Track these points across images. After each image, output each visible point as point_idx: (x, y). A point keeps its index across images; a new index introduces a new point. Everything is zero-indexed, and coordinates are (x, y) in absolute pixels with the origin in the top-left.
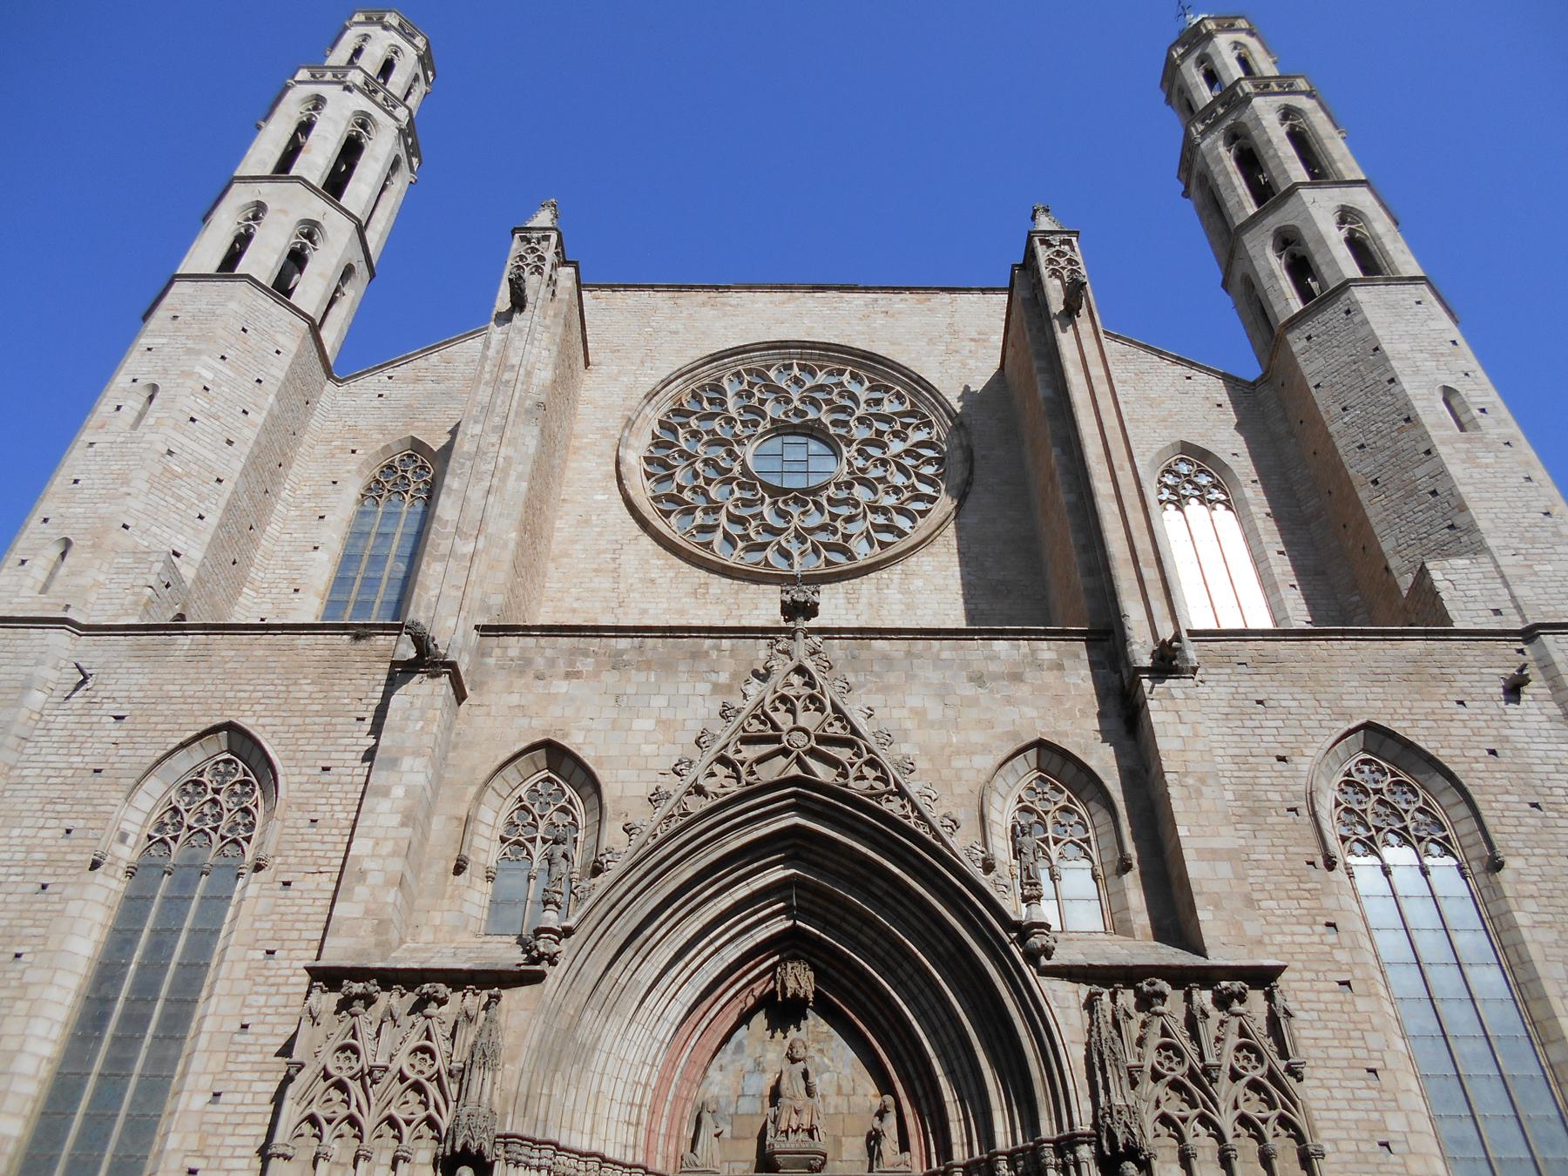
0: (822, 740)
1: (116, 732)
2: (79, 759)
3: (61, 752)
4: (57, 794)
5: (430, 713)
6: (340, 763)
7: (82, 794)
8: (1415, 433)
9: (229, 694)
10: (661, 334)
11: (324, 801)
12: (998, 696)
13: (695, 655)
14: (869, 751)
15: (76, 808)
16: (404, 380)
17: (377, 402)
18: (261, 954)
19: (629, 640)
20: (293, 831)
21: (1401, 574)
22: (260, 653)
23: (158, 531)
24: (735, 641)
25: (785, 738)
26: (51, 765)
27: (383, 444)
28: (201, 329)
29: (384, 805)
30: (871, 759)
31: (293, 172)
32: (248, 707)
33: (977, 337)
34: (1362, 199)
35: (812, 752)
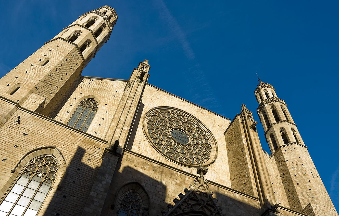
0: (207, 204)
1: (23, 138)
2: (12, 141)
3: (7, 137)
4: (4, 148)
5: (114, 165)
6: (82, 169)
7: (11, 151)
8: (307, 176)
9: (55, 140)
10: (155, 98)
11: (77, 177)
12: (237, 206)
13: (172, 174)
14: (218, 211)
15: (8, 154)
16: (96, 83)
17: (89, 85)
18: (55, 214)
19: (157, 165)
20: (68, 182)
21: (302, 204)
22: (65, 133)
23: (42, 92)
24: (181, 174)
25: (199, 201)
26: (3, 139)
27: (88, 95)
28: (64, 51)
29: (100, 185)
30: (218, 212)
31: (89, 28)
32: (60, 145)
33: (219, 125)
34: (295, 128)
35: (205, 206)
